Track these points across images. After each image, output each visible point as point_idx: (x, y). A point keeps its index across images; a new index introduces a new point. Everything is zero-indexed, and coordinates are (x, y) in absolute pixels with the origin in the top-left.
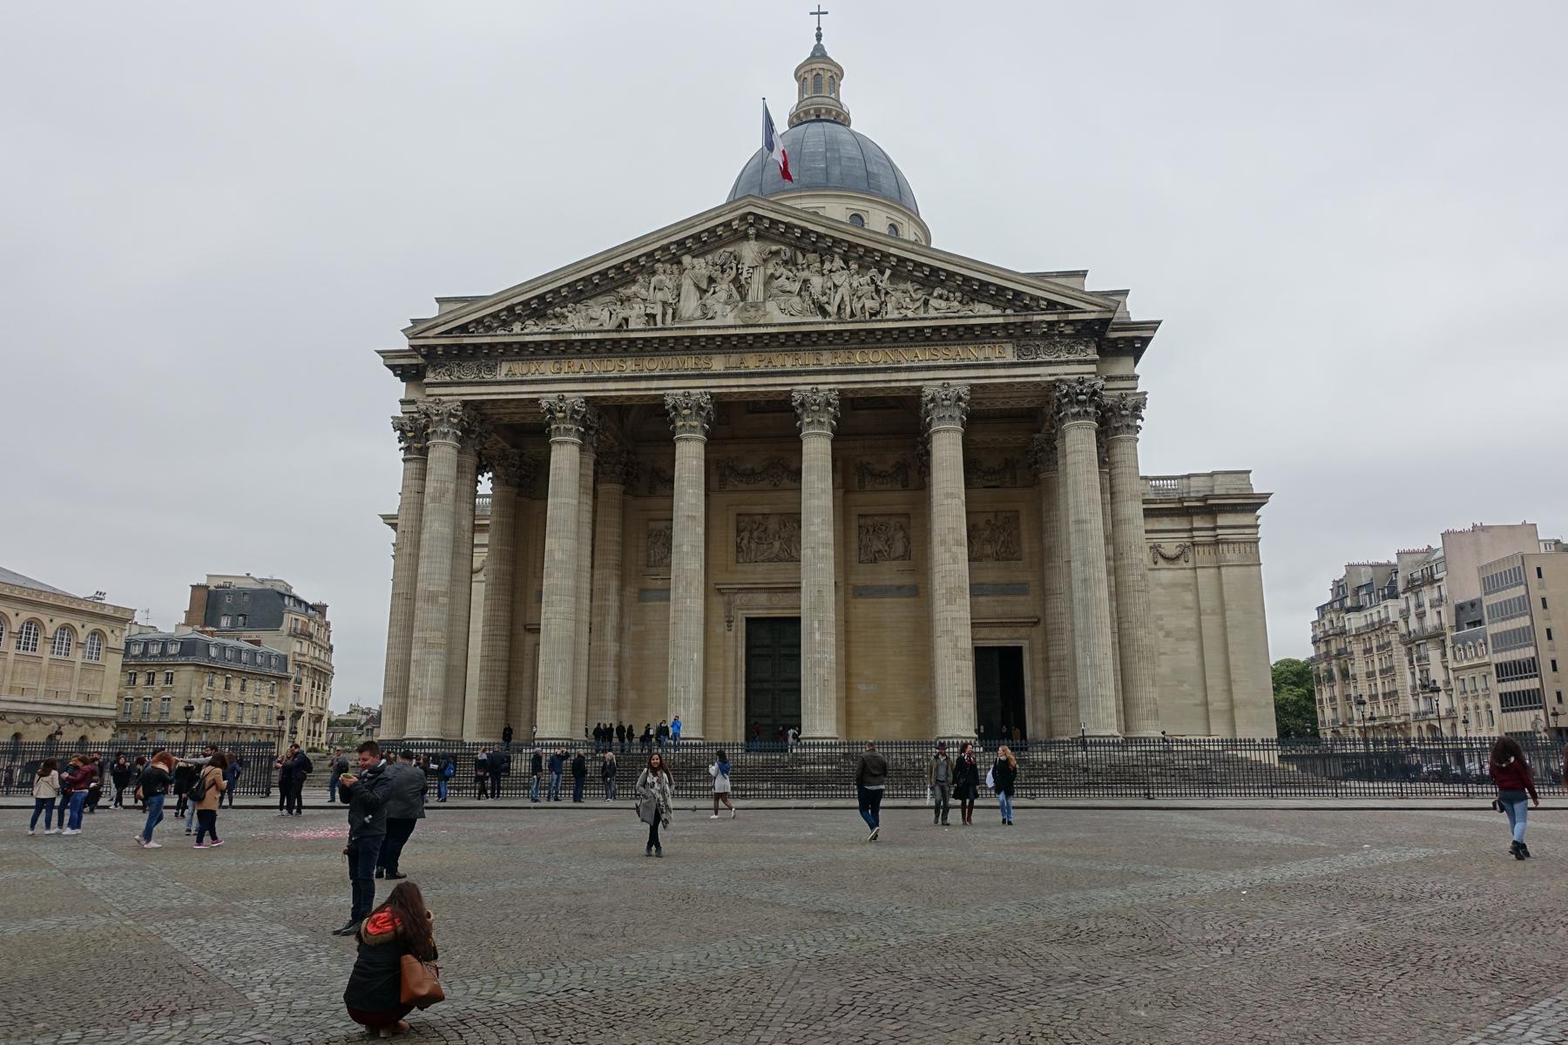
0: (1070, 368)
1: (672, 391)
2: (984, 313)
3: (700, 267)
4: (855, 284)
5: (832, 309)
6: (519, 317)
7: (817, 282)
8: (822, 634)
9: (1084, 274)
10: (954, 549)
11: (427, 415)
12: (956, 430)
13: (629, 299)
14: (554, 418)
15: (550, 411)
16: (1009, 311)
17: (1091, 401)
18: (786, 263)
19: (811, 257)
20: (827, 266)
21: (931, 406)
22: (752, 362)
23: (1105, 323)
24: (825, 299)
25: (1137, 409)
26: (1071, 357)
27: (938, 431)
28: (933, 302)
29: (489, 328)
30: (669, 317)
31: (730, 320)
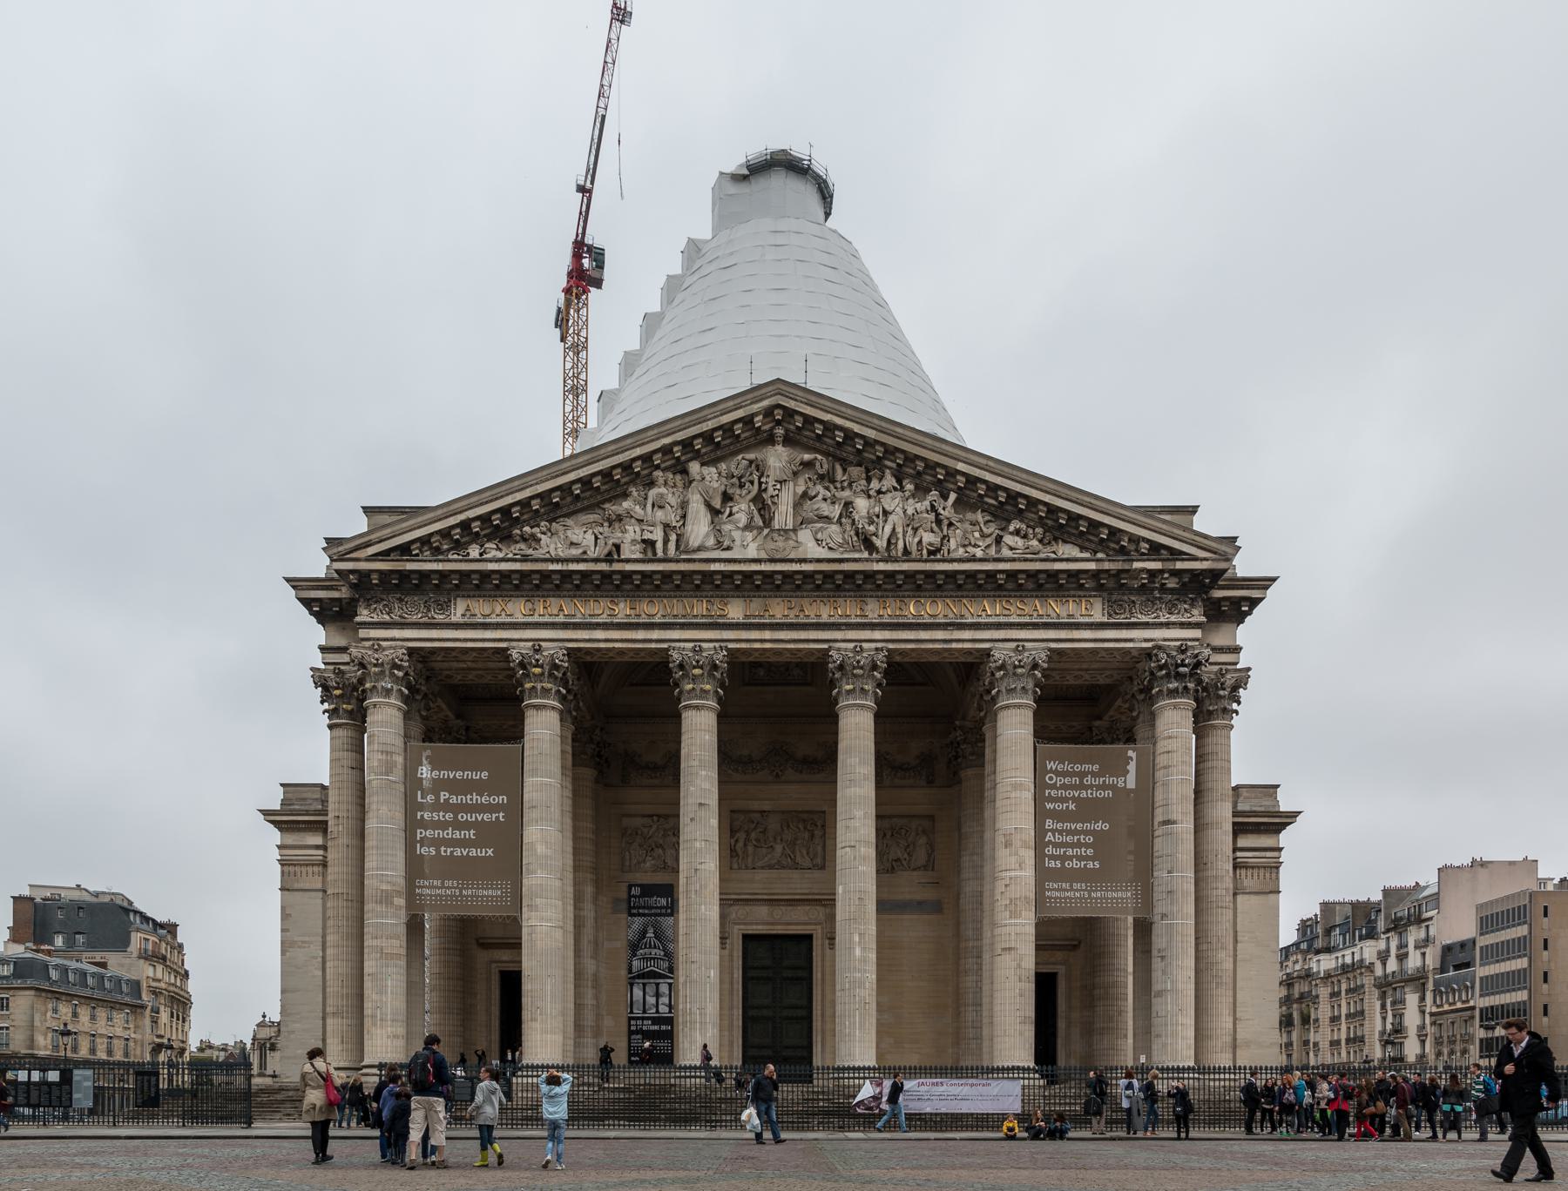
0: (1166, 631)
1: (680, 642)
2: (1070, 557)
3: (710, 477)
4: (910, 511)
5: (880, 543)
6: (475, 538)
7: (862, 504)
8: (864, 949)
9: (1192, 510)
10: (1022, 852)
11: (362, 665)
12: (1027, 706)
13: (620, 518)
14: (526, 675)
15: (522, 665)
16: (1100, 555)
17: (1191, 675)
18: (821, 477)
19: (855, 471)
20: (875, 485)
21: (999, 674)
22: (779, 610)
23: (1216, 575)
24: (872, 528)
25: (1242, 679)
26: (1173, 618)
27: (1007, 707)
28: (1009, 540)
29: (437, 551)
30: (672, 546)
31: (752, 552)
